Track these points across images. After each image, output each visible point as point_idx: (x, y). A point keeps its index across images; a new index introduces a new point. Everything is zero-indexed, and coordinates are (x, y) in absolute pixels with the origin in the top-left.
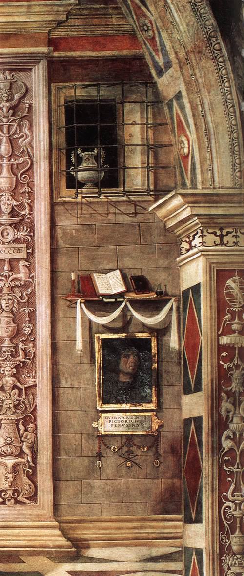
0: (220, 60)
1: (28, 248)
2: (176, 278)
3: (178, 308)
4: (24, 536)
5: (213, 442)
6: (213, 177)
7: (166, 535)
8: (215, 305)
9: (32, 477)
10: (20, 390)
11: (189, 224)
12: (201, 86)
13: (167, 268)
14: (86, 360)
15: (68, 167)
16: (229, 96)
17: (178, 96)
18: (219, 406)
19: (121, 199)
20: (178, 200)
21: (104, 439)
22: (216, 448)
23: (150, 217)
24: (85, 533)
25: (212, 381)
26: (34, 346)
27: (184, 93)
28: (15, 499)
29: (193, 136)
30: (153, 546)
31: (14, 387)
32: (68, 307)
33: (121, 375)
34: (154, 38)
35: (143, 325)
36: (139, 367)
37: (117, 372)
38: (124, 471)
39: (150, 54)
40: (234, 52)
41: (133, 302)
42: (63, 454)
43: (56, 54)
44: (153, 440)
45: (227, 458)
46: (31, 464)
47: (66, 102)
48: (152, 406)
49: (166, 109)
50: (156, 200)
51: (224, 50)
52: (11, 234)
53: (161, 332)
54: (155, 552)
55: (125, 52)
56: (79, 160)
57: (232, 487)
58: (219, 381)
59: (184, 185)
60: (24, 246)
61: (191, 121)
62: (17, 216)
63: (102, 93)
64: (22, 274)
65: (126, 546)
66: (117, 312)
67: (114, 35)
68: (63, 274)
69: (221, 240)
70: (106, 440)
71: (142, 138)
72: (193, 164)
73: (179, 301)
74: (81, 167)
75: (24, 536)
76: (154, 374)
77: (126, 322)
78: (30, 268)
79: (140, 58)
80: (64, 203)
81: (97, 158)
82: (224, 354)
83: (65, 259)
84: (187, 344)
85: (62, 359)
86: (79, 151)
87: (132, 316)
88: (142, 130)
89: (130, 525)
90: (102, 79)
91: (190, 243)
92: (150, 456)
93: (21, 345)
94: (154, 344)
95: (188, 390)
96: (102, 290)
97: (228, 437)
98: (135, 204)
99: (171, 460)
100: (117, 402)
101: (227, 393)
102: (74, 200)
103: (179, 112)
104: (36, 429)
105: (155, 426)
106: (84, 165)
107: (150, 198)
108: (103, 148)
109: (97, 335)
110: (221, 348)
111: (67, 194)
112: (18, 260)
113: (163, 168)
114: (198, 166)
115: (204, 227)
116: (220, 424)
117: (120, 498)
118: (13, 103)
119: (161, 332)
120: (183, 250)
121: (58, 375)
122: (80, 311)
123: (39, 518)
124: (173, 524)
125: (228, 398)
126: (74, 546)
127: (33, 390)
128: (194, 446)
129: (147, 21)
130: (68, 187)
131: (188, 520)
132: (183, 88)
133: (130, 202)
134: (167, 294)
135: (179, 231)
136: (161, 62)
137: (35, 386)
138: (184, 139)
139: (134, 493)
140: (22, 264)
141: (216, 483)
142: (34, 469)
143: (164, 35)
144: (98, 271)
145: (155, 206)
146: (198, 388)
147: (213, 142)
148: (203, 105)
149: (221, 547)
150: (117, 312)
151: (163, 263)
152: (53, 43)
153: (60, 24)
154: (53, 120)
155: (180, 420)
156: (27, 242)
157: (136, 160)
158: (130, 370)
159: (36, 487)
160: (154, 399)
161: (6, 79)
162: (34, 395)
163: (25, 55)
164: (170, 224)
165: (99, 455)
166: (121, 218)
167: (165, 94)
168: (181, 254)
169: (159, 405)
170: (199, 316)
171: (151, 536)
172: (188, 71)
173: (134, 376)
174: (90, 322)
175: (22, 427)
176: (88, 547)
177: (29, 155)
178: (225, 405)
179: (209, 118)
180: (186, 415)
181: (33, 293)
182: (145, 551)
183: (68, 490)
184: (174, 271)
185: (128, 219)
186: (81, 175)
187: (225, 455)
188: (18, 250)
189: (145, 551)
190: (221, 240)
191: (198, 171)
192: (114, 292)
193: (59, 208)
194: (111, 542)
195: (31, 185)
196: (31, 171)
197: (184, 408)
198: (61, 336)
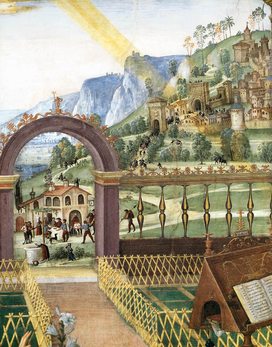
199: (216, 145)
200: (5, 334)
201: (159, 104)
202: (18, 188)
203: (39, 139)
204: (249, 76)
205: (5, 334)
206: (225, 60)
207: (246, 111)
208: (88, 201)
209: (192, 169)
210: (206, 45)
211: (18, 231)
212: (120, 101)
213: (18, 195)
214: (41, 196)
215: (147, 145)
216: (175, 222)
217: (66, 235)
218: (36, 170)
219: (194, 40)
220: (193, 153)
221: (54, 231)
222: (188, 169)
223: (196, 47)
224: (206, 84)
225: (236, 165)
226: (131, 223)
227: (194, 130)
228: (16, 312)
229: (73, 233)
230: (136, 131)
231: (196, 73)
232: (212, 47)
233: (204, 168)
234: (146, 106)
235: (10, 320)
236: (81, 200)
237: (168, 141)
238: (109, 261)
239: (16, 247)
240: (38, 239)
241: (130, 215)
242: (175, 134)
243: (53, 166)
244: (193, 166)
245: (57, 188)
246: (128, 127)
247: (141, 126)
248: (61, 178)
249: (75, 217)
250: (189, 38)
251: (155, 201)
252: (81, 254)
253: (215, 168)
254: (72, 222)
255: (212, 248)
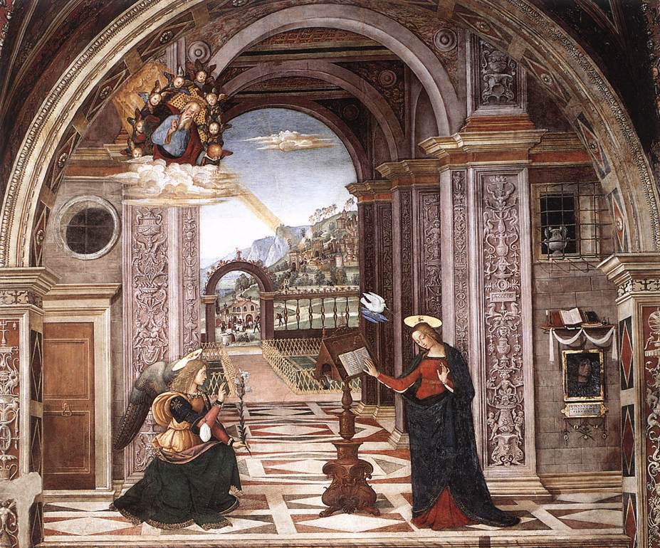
0: (644, 166)
1: (517, 294)
2: (615, 313)
3: (617, 333)
4: (517, 487)
5: (641, 421)
6: (639, 245)
7: (612, 485)
8: (641, 330)
9: (521, 447)
10: (513, 388)
11: (624, 276)
12: (630, 184)
13: (610, 306)
14: (556, 368)
15: (543, 240)
16: (650, 191)
17: (615, 191)
18: (646, 397)
19: (578, 260)
20: (616, 261)
21: (569, 420)
22: (644, 425)
23: (598, 272)
24: (556, 485)
25: (640, 380)
26: (522, 359)
27: (619, 189)
28: (510, 462)
29: (625, 218)
30: (603, 492)
31: (509, 387)
32: (544, 333)
33: (580, 377)
34: (598, 153)
35: (594, 344)
36: (591, 372)
37: (577, 375)
38: (583, 441)
39: (596, 163)
40: (654, 160)
41: (585, 329)
42: (542, 431)
43: (534, 164)
44: (601, 420)
45: (652, 432)
46: (521, 438)
47: (541, 196)
48: (601, 398)
49: (607, 199)
50: (601, 261)
51: (646, 161)
52: (506, 285)
53: (606, 349)
54: (604, 496)
55: (580, 162)
56: (550, 235)
57: (657, 452)
58: (646, 380)
59: (620, 251)
60: (515, 292)
61: (624, 207)
62: (510, 273)
63: (564, 190)
64: (513, 312)
65: (585, 492)
66: (576, 337)
67: (571, 152)
68: (541, 311)
69: (646, 287)
70: (571, 422)
71: (592, 220)
72: (626, 236)
73: (617, 328)
74: (551, 240)
75: (517, 487)
76: (602, 377)
77: (582, 343)
78: (519, 307)
79: (590, 166)
80: (541, 264)
81: (561, 233)
82: (649, 363)
83: (541, 301)
84: (623, 357)
85: (540, 367)
86: (550, 229)
87: (586, 338)
88: (591, 214)
89: (588, 478)
90: (565, 180)
91: (624, 289)
92: (600, 431)
93: (513, 359)
94: (601, 357)
95: (624, 387)
96: (566, 322)
97: (653, 418)
98: (587, 263)
99: (613, 434)
100: (577, 396)
101: (651, 388)
102: (547, 262)
103: (616, 202)
104: (524, 415)
105: (603, 412)
106: (553, 238)
107: (598, 260)
108: (567, 227)
109: (563, 352)
110: (646, 359)
111: (542, 258)
112: (510, 302)
113: (606, 239)
114: (629, 237)
115: (634, 279)
116: (646, 410)
117: (580, 460)
118: (506, 197)
119: (606, 349)
120: (620, 294)
121: (538, 378)
122: (552, 335)
123: (526, 474)
124: (616, 477)
125: (653, 392)
126: (550, 493)
127: (521, 389)
128: (628, 425)
129: (594, 142)
130: (543, 253)
131: (626, 474)
132: (618, 186)
133: (585, 262)
134: (609, 324)
135: (616, 282)
136: (604, 170)
137: (523, 386)
138: (619, 219)
139: (589, 457)
140: (513, 304)
141: (644, 449)
142: (523, 442)
143: (605, 151)
144: (563, 309)
145: (600, 265)
146: (631, 386)
147: (639, 221)
148: (631, 197)
149: (649, 492)
150: (576, 337)
151: (607, 303)
152: (530, 157)
153: (536, 144)
154: (532, 208)
155: (619, 408)
156: (517, 290)
157: (588, 234)
158: (585, 374)
159: (524, 455)
160: (602, 393)
161: (501, 181)
162: (522, 392)
163: (513, 165)
164: (611, 277)
165: (566, 432)
166: (579, 273)
167: (607, 190)
168: (618, 296)
169: (605, 397)
170: (631, 338)
171: (601, 485)
172: (621, 174)
173: (588, 378)
174: (559, 342)
175: (513, 412)
176: (560, 493)
177: (516, 231)
178: (650, 397)
179: (636, 205)
180: (622, 405)
181: (521, 324)
182: (597, 495)
183: (546, 455)
184: (614, 308)
185: (583, 274)
186: (551, 245)
187: (650, 430)
188: (510, 296)
189: (597, 495)
190: (646, 287)
191: (629, 241)
192: (575, 323)
193: (536, 267)
194: (575, 490)
195: (518, 252)
196: (517, 243)
197: (622, 399)
198: (540, 352)
199: (328, 277)
200: (211, 384)
201: (295, 254)
202: (217, 302)
203: (227, 275)
204: (345, 236)
205: (211, 384)
206: (332, 228)
207: (344, 257)
208: (256, 309)
209: (315, 290)
210: (321, 220)
211: (217, 326)
212: (273, 253)
213: (217, 305)
214: (230, 307)
215: (289, 277)
216: (305, 320)
217: (245, 328)
218: (227, 292)
219: (314, 217)
220: (315, 281)
221: (237, 326)
222: (312, 290)
223: (316, 221)
224: (322, 242)
225: (339, 287)
226: (280, 321)
227: (316, 268)
228: (217, 371)
229: (248, 327)
230: (283, 269)
231: (315, 235)
232: (325, 221)
233: (321, 289)
234: (288, 255)
235: (214, 376)
236: (252, 309)
237: (300, 275)
238: (269, 342)
239: (216, 335)
240: (229, 331)
241: (280, 317)
242: (304, 270)
243: (237, 290)
244: (315, 288)
245: (239, 302)
246: (278, 267)
247: (286, 266)
248: (241, 296)
249: (249, 318)
250: (312, 216)
251: (294, 308)
252: (253, 339)
253: (327, 289)
254: (247, 322)
255: (326, 334)
